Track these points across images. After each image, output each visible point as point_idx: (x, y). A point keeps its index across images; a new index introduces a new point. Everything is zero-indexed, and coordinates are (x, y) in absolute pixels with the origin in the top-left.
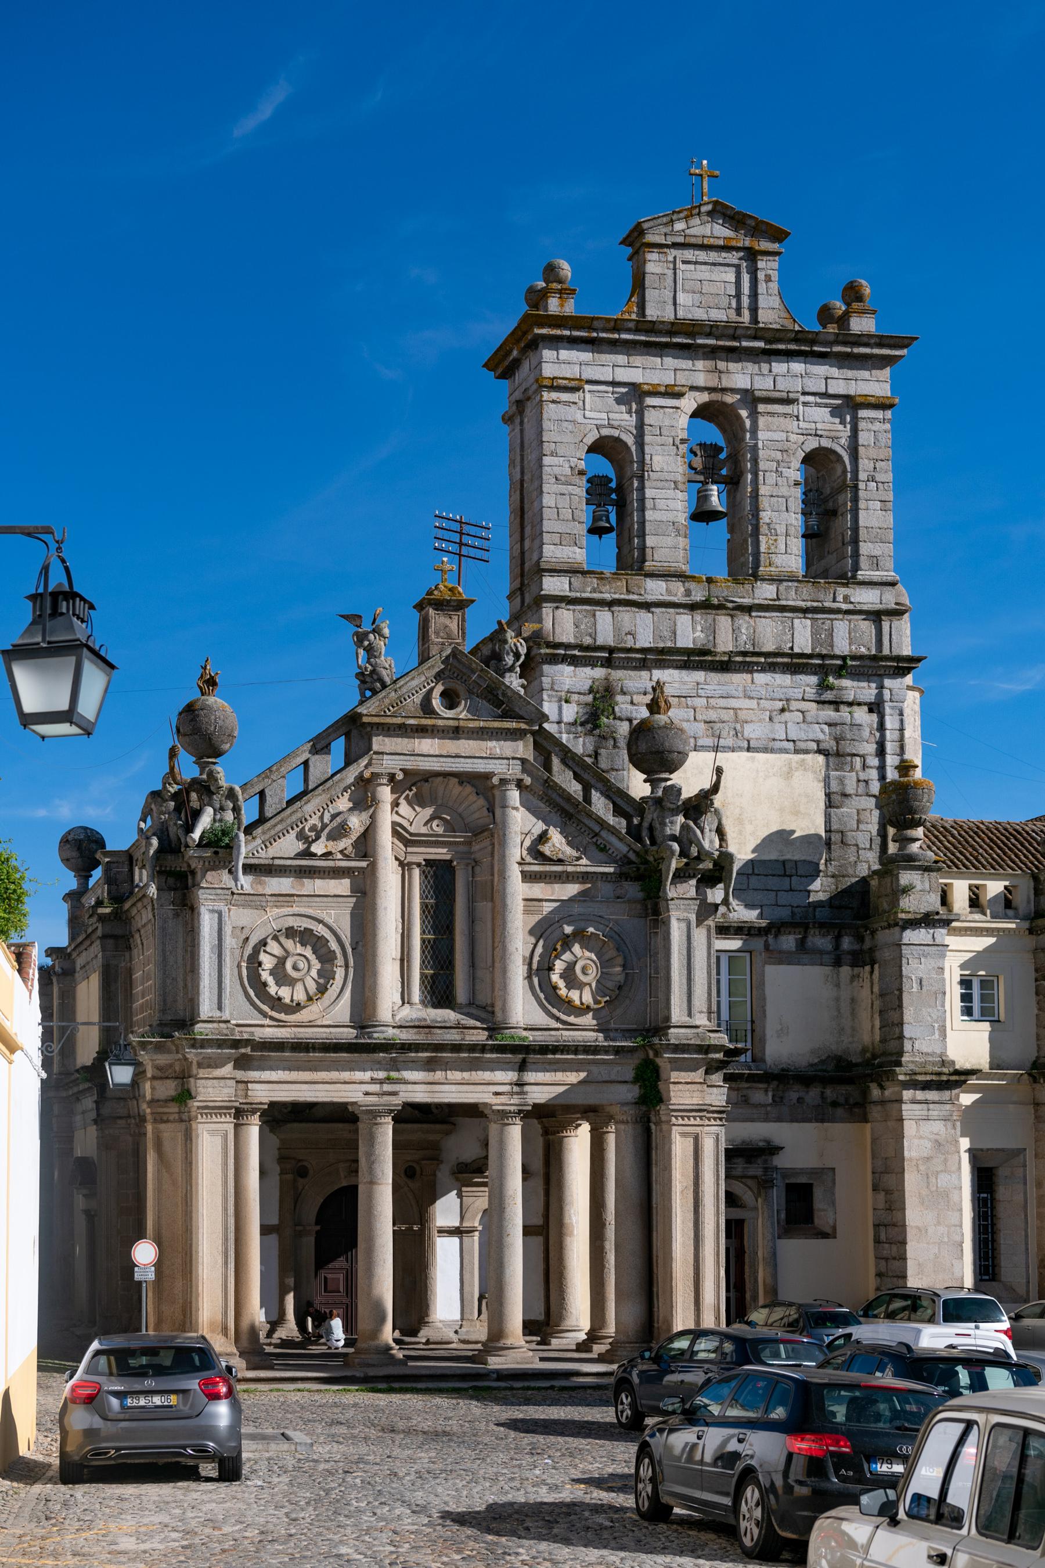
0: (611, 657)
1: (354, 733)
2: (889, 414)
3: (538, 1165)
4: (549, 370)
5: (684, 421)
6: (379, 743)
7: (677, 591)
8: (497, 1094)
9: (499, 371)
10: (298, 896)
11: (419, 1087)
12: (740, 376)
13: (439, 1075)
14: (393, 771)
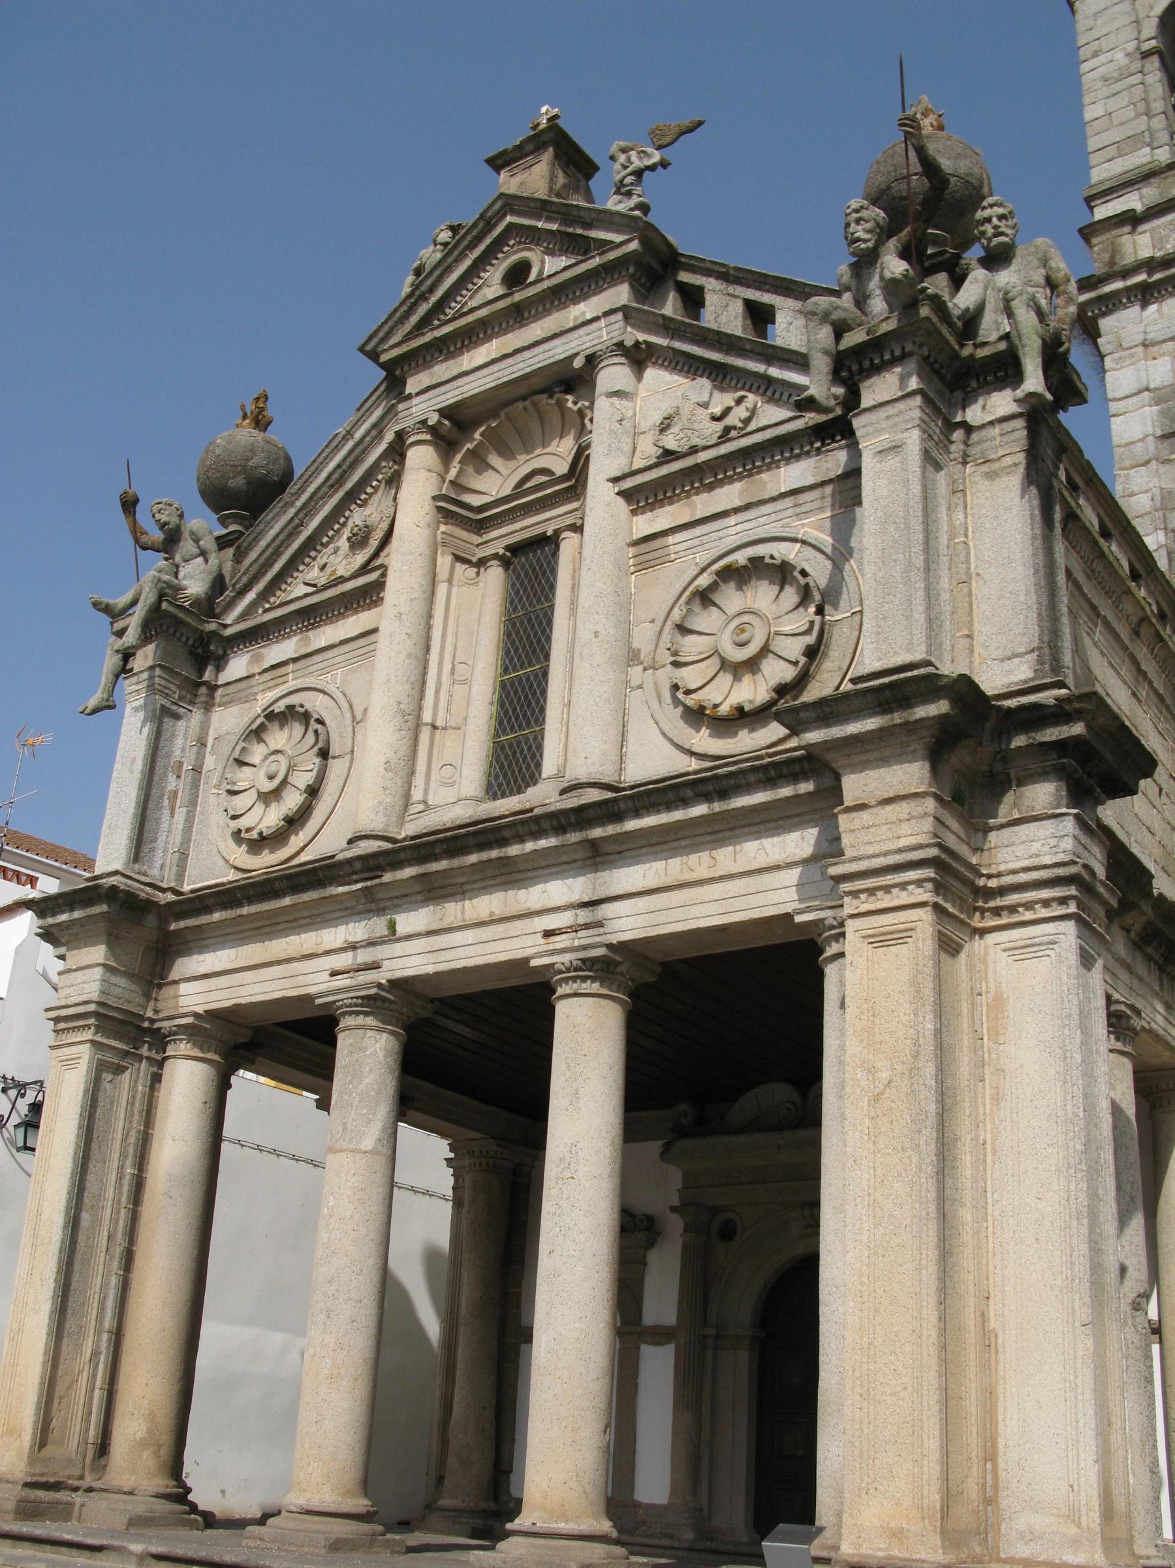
8: (548, 934)
10: (294, 660)
13: (452, 911)
14: (423, 417)
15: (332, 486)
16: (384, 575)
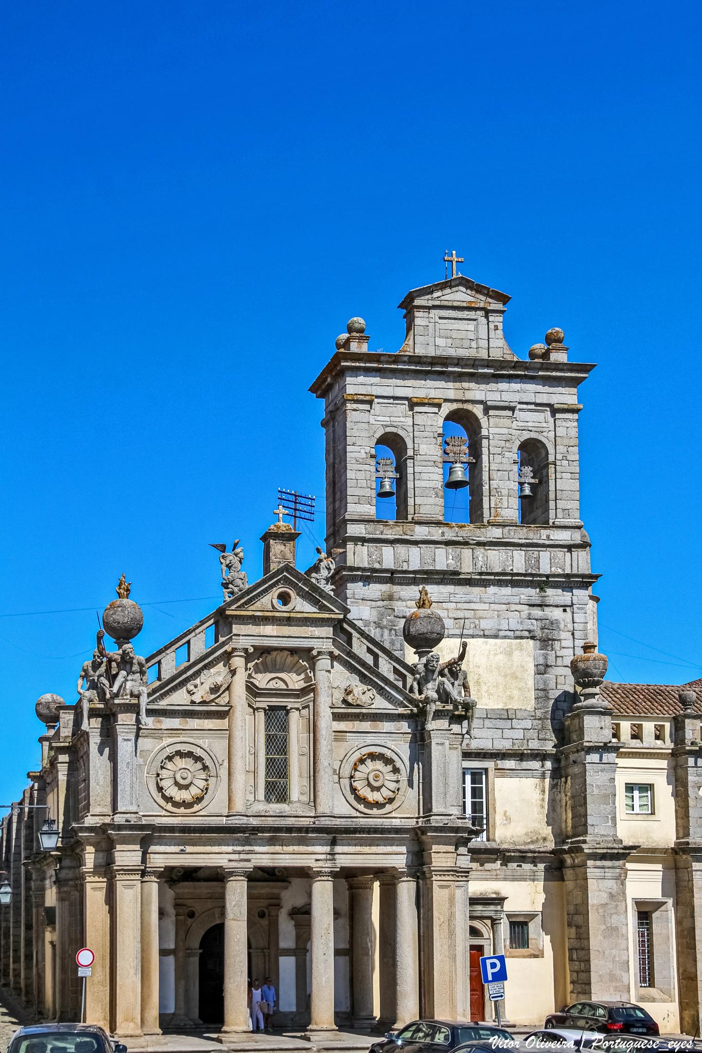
0: (393, 577)
1: (221, 622)
2: (576, 416)
3: (345, 908)
4: (350, 390)
5: (441, 422)
6: (236, 629)
7: (436, 533)
8: (317, 860)
9: (319, 392)
11: (264, 856)
12: (477, 391)
13: (278, 849)
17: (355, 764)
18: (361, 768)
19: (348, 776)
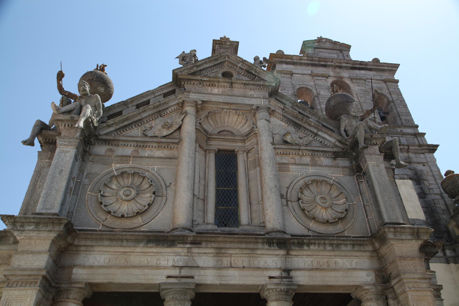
8: (270, 278)
15: (154, 107)
16: (179, 142)
17: (301, 189)
18: (306, 192)
19: (297, 199)
